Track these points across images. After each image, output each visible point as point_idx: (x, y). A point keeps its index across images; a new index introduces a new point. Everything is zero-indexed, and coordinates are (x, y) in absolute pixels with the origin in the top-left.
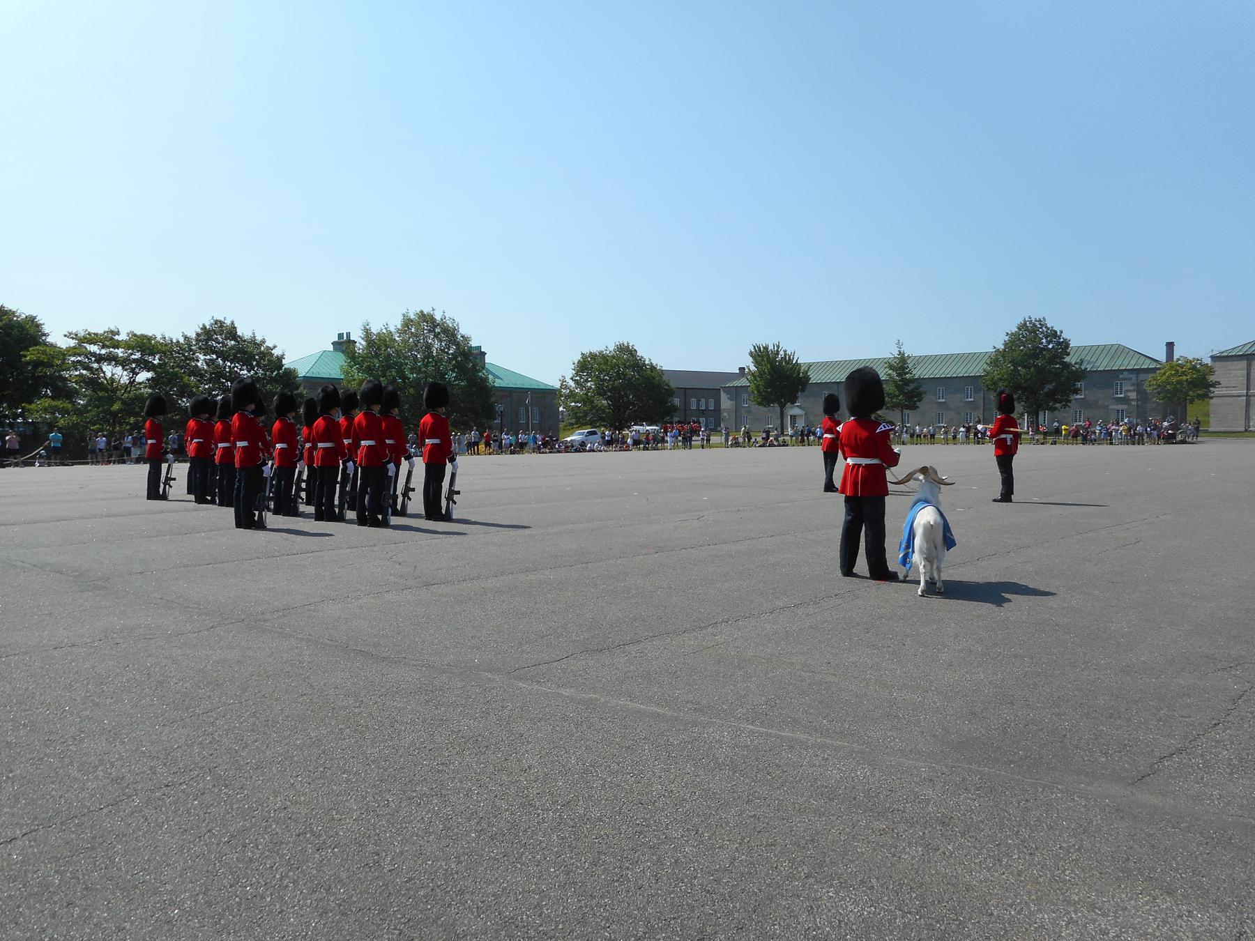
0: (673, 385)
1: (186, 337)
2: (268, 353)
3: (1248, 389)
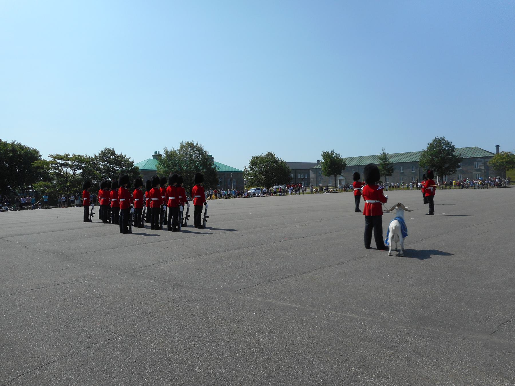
0: (290, 168)
1: (95, 156)
2: (127, 160)
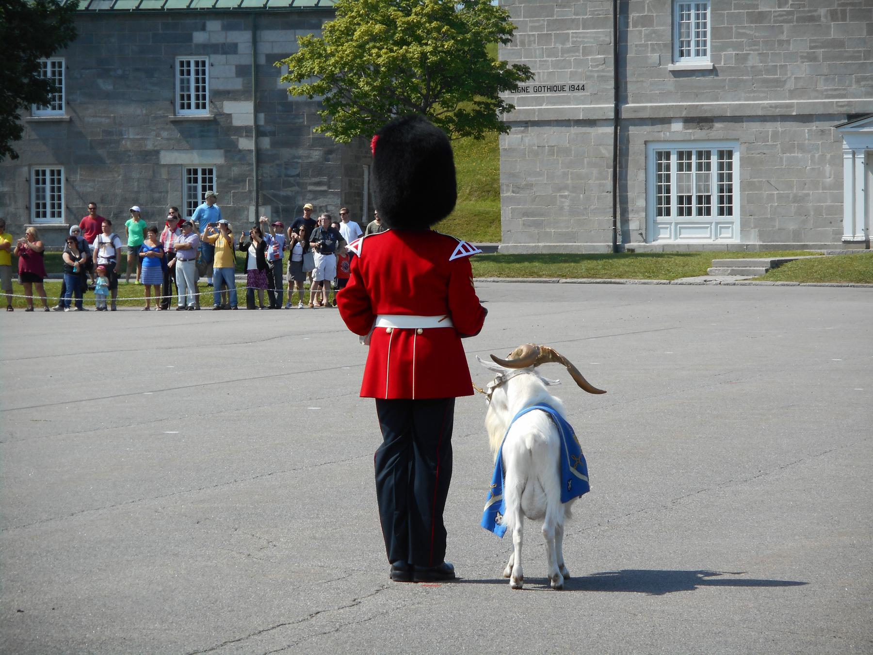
3: (619, 97)
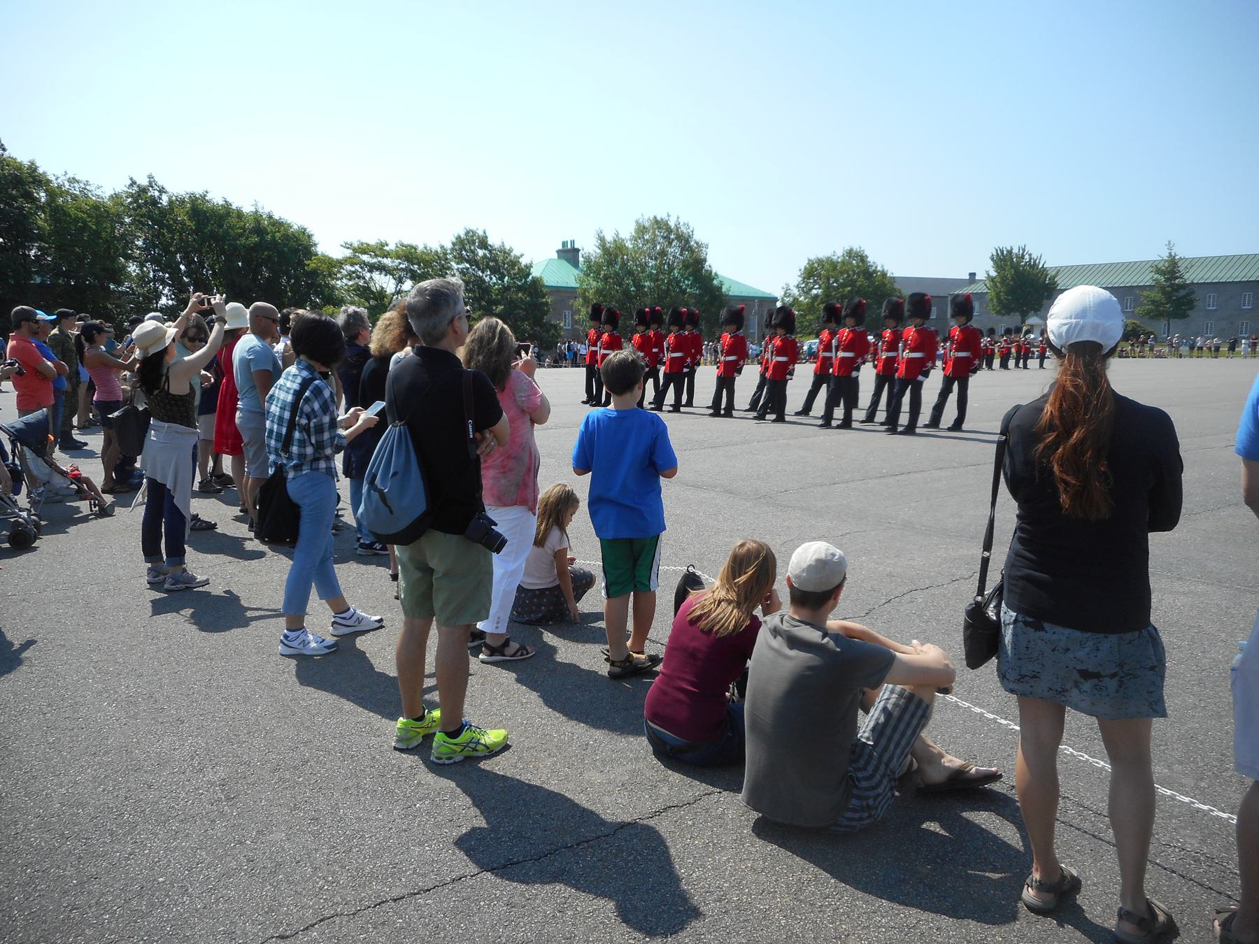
1: (442, 247)
2: (514, 263)
